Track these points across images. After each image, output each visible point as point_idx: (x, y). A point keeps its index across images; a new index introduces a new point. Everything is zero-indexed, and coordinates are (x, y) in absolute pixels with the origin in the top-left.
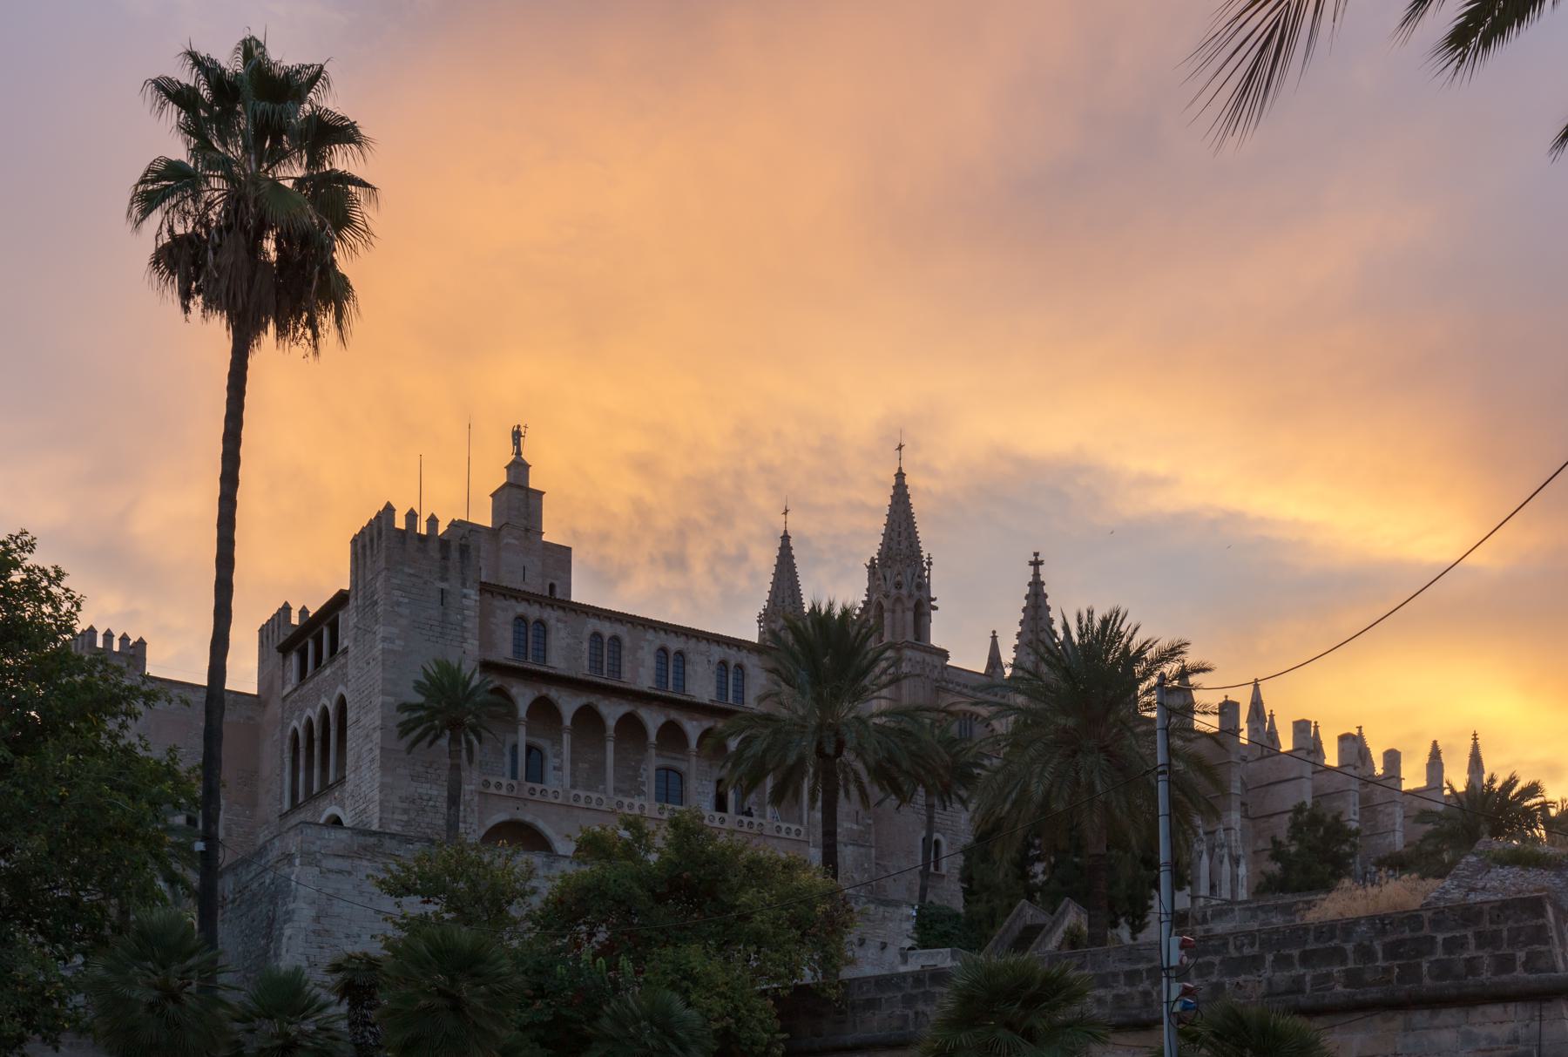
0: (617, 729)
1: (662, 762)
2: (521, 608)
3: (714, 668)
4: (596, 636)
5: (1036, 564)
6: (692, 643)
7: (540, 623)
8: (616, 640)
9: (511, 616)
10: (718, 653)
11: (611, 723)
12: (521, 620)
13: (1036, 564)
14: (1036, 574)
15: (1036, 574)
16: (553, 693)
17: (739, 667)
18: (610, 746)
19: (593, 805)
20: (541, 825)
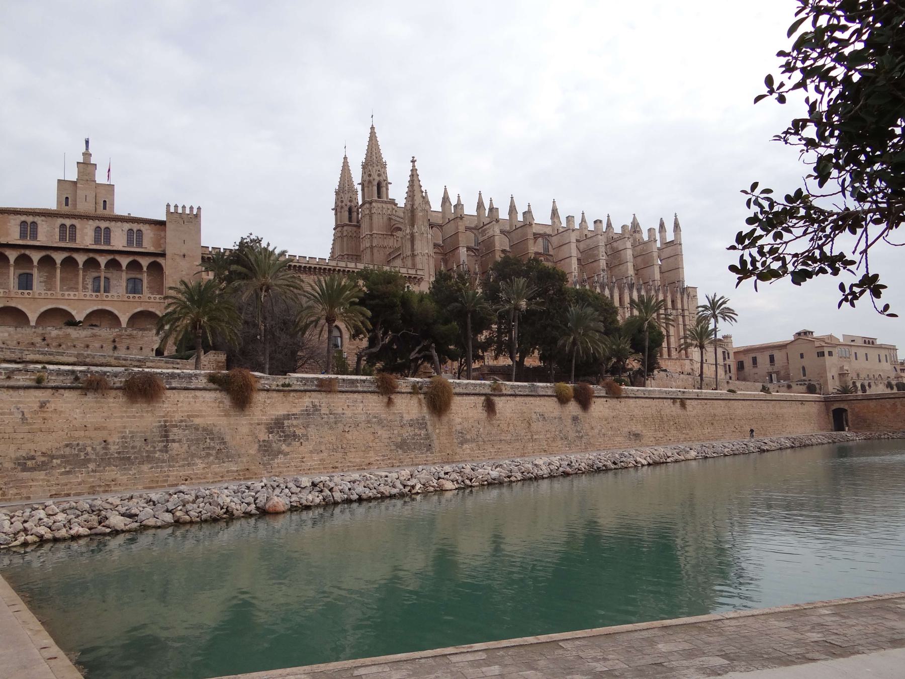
0: (62, 264)
2: (23, 218)
3: (125, 233)
4: (63, 226)
5: (413, 161)
6: (113, 223)
7: (34, 223)
8: (73, 227)
9: (18, 222)
10: (127, 226)
11: (58, 262)
12: (24, 223)
13: (413, 161)
14: (414, 166)
15: (414, 166)
16: (27, 252)
17: (139, 231)
18: (58, 271)
19: (49, 296)
20: (20, 307)
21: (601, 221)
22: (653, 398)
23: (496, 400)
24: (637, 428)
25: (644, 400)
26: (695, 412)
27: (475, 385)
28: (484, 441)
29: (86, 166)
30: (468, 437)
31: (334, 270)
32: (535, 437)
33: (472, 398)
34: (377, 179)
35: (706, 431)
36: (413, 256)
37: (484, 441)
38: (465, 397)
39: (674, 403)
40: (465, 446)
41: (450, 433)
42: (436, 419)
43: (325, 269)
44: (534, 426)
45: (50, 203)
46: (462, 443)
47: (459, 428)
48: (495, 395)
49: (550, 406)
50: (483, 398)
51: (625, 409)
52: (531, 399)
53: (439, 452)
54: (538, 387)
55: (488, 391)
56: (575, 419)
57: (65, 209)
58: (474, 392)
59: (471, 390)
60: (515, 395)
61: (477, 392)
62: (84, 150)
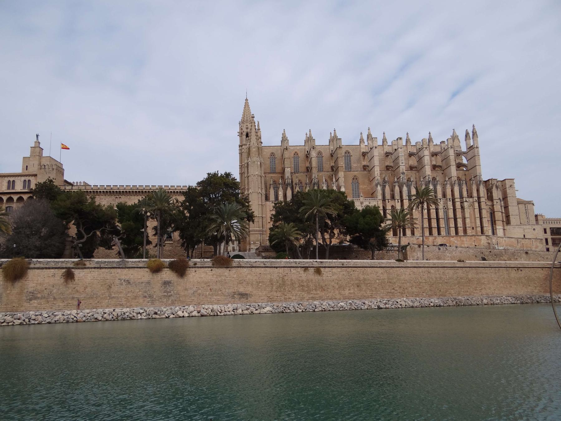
1: (7, 206)
10: (23, 179)
21: (401, 139)
22: (277, 267)
23: (77, 272)
24: (249, 290)
25: (263, 269)
26: (335, 277)
27: (58, 262)
28: (55, 299)
29: (37, 149)
30: (39, 295)
31: (142, 192)
32: (113, 296)
33: (52, 270)
34: (245, 130)
35: (347, 292)
36: (248, 177)
37: (55, 299)
38: (44, 270)
39: (305, 271)
40: (33, 301)
41: (21, 293)
42: (9, 284)
43: (136, 192)
44: (114, 289)
45: (19, 170)
46: (31, 300)
47: (31, 290)
48: (79, 268)
49: (144, 275)
50: (64, 270)
51: (235, 276)
52: (119, 270)
53: (6, 305)
54: (128, 262)
55: (72, 266)
56: (166, 283)
57: (26, 172)
58: (54, 266)
59: (52, 265)
60: (101, 268)
61: (59, 266)
62: (36, 140)
